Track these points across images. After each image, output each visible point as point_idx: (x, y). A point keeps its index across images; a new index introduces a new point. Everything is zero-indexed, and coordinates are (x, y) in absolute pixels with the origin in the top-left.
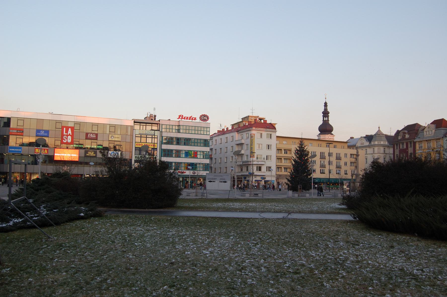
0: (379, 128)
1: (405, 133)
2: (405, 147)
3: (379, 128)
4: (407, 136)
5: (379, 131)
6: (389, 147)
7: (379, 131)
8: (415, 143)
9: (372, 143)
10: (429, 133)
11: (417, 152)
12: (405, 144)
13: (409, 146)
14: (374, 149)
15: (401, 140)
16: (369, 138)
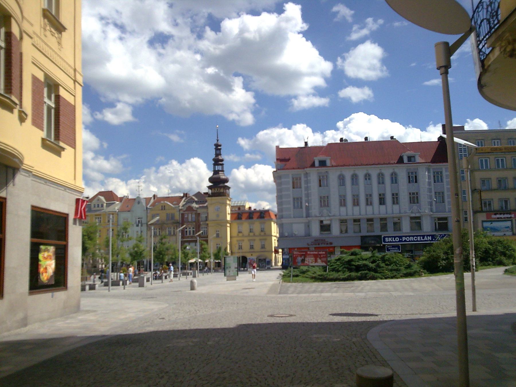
10: (98, 206)
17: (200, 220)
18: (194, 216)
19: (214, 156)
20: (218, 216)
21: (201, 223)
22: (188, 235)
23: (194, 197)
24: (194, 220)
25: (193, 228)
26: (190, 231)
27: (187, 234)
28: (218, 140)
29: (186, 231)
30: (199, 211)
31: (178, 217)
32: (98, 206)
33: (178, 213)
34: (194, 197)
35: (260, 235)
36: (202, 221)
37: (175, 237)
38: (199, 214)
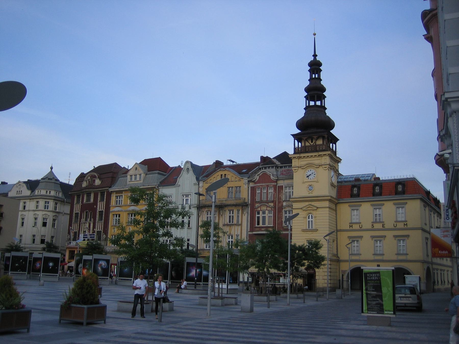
0: (52, 168)
1: (95, 177)
2: (92, 200)
3: (52, 168)
4: (98, 182)
5: (51, 173)
6: (64, 202)
7: (51, 173)
8: (109, 195)
9: (36, 192)
10: (135, 178)
11: (112, 209)
12: (92, 196)
13: (99, 199)
14: (37, 202)
15: (86, 188)
16: (32, 185)
17: (283, 198)
18: (271, 191)
19: (308, 83)
20: (310, 188)
21: (284, 204)
22: (261, 225)
23: (275, 161)
24: (270, 197)
25: (269, 212)
26: (264, 218)
27: (258, 224)
28: (315, 56)
29: (258, 218)
30: (280, 183)
31: (245, 194)
32: (135, 178)
33: (246, 186)
34: (275, 161)
35: (395, 228)
36: (284, 201)
37: (239, 228)
38: (281, 187)
